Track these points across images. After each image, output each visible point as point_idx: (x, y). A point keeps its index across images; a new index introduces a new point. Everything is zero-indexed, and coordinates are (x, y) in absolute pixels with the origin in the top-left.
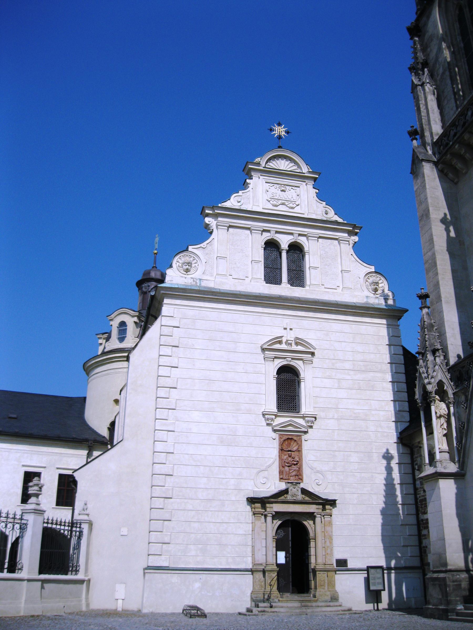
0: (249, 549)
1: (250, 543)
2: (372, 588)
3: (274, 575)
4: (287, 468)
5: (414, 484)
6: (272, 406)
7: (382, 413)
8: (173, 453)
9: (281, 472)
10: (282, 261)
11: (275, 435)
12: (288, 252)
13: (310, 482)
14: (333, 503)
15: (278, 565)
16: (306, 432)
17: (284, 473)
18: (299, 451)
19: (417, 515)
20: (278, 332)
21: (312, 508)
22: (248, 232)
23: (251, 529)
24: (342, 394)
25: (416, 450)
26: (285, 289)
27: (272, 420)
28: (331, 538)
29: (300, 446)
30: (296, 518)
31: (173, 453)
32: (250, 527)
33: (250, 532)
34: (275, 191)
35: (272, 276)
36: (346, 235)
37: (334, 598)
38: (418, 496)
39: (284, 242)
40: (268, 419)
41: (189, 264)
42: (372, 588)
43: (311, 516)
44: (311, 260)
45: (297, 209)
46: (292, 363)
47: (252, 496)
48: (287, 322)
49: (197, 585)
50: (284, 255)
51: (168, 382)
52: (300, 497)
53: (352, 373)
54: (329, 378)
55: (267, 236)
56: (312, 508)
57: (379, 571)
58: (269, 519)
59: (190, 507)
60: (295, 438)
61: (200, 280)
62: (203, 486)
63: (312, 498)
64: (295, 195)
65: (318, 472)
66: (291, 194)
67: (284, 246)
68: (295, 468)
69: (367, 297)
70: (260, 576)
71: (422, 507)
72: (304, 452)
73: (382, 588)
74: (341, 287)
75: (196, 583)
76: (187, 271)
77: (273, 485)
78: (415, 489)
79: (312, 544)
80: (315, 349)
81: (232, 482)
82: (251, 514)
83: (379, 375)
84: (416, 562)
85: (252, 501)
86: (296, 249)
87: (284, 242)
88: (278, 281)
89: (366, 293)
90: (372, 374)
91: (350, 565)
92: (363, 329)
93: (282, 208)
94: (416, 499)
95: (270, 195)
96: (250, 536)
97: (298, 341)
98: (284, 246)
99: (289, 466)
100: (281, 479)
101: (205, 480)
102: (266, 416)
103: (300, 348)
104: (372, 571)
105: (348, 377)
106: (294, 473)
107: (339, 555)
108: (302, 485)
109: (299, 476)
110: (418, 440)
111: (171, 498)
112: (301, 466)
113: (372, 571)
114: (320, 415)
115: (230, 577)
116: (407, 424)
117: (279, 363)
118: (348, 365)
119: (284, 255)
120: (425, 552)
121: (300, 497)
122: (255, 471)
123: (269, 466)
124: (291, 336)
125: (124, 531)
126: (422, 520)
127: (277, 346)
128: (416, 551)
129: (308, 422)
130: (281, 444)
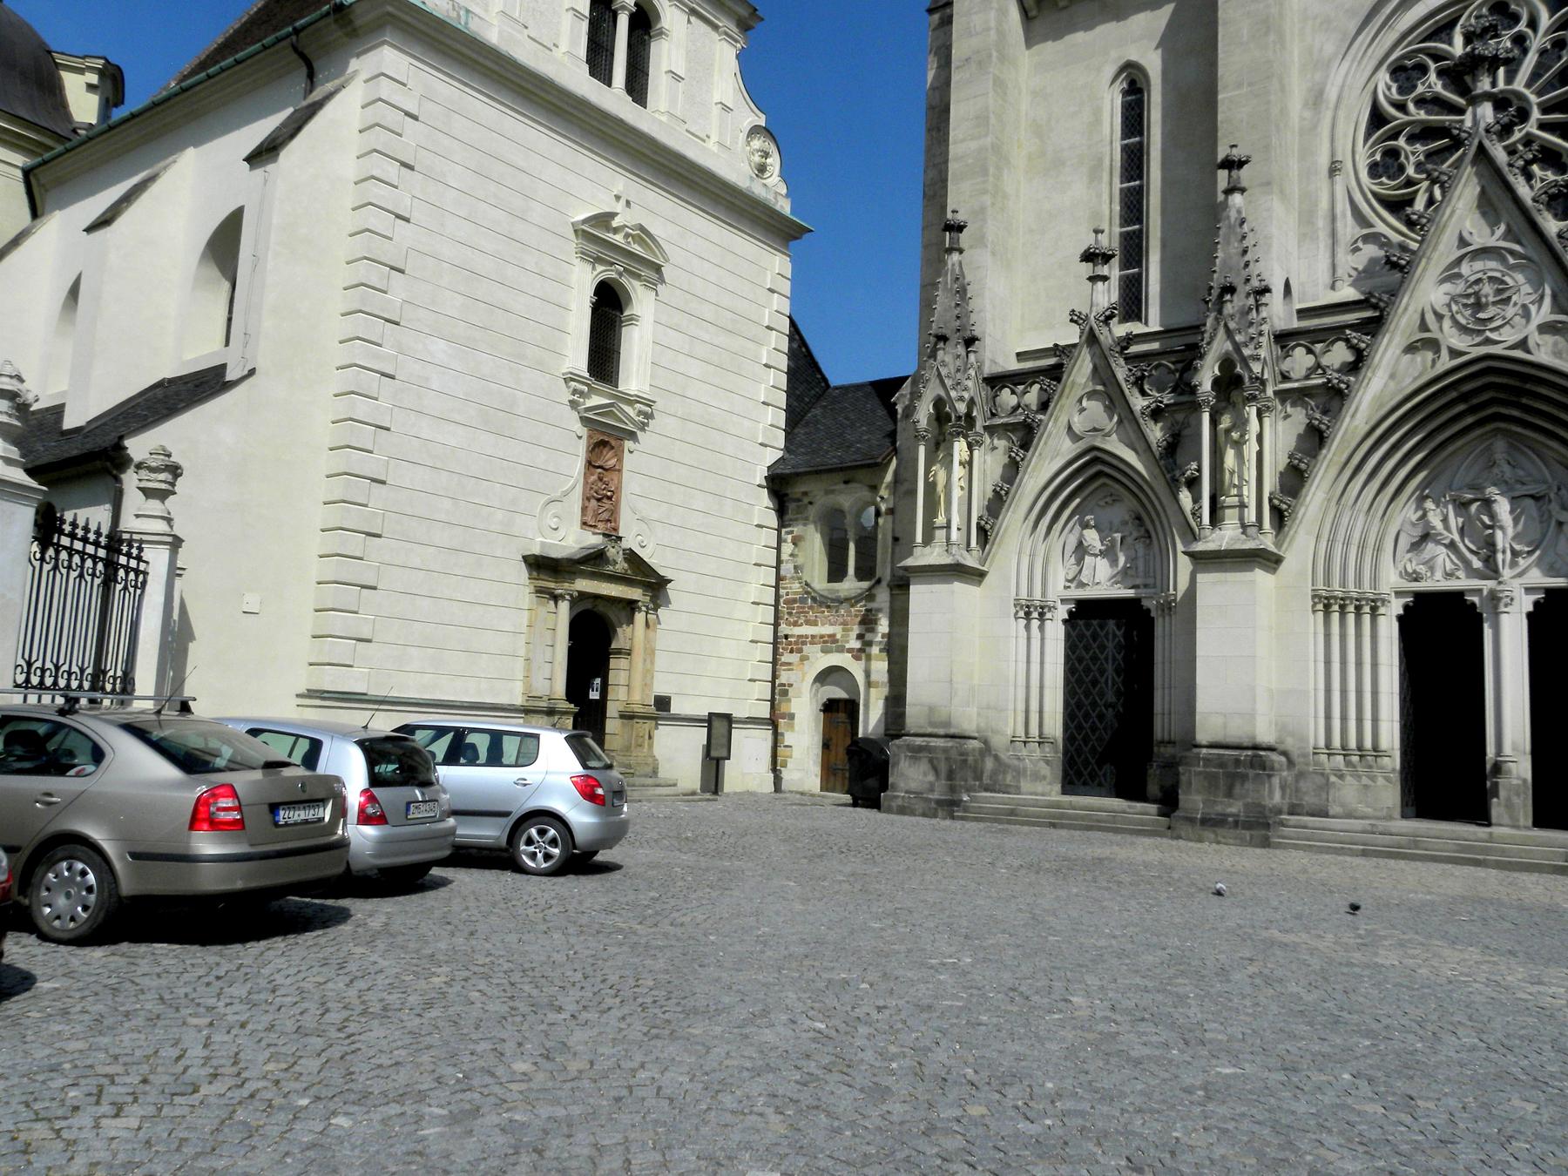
0: (520, 664)
1: (522, 652)
2: (714, 754)
4: (594, 503)
5: (778, 568)
7: (747, 423)
8: (388, 429)
9: (584, 509)
11: (584, 432)
16: (632, 436)
17: (590, 513)
19: (776, 625)
21: (634, 593)
23: (526, 623)
25: (792, 506)
26: (613, 98)
27: (581, 394)
29: (620, 460)
30: (601, 608)
31: (388, 429)
33: (525, 629)
38: (782, 592)
40: (575, 392)
42: (714, 754)
43: (631, 606)
46: (624, 280)
47: (536, 551)
52: (621, 566)
53: (712, 329)
56: (634, 593)
57: (725, 723)
58: (564, 607)
59: (416, 562)
60: (613, 443)
61: (468, 11)
62: (443, 517)
68: (607, 504)
71: (790, 614)
73: (724, 754)
74: (714, 138)
78: (779, 578)
80: (667, 261)
81: (499, 515)
82: (528, 590)
83: (750, 345)
84: (764, 711)
91: (675, 709)
94: (777, 596)
96: (522, 639)
99: (599, 500)
100: (584, 523)
101: (447, 504)
102: (573, 384)
103: (636, 248)
105: (706, 337)
106: (605, 516)
107: (660, 689)
108: (625, 544)
110: (803, 489)
111: (379, 536)
112: (618, 501)
113: (716, 723)
116: (780, 454)
117: (602, 272)
118: (708, 312)
120: (785, 693)
123: (566, 494)
125: (252, 601)
126: (786, 637)
128: (765, 690)
129: (640, 413)
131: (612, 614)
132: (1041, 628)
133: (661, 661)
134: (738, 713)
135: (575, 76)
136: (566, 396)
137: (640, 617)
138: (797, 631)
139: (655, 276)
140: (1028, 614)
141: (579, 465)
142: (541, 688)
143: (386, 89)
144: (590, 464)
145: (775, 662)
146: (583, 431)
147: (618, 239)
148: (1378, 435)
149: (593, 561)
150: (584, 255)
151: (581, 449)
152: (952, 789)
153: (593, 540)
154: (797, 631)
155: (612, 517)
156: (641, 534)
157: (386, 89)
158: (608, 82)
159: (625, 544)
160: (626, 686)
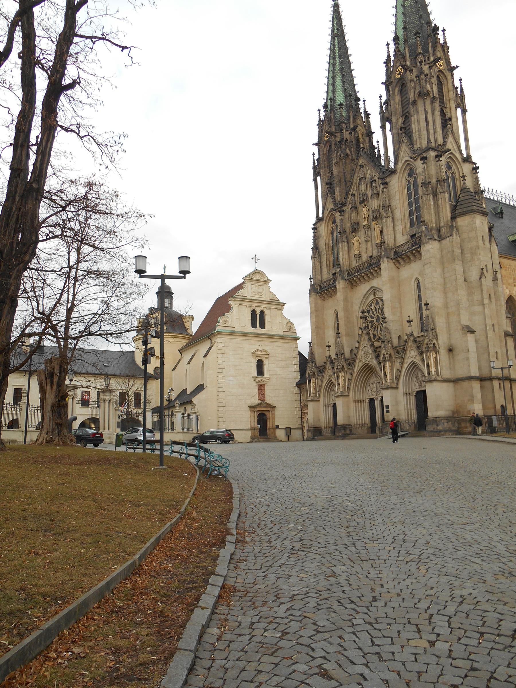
6: (255, 374)
10: (258, 319)
13: (268, 400)
14: (275, 407)
21: (269, 409)
24: (278, 369)
34: (255, 288)
36: (280, 307)
37: (276, 437)
43: (269, 411)
44: (267, 318)
48: (260, 343)
50: (258, 316)
51: (222, 367)
52: (265, 405)
54: (274, 363)
56: (269, 409)
58: (255, 413)
63: (269, 405)
66: (260, 290)
67: (258, 312)
70: (253, 431)
77: (256, 401)
79: (268, 421)
85: (250, 407)
86: (262, 313)
88: (256, 327)
92: (285, 345)
95: (253, 290)
97: (264, 351)
98: (258, 312)
103: (264, 353)
109: (264, 398)
114: (271, 377)
115: (244, 432)
117: (258, 359)
118: (280, 359)
119: (258, 316)
121: (265, 405)
124: (261, 349)
127: (257, 353)
130: (258, 388)
131: (266, 413)
132: (364, 404)
133: (276, 419)
135: (251, 330)
137: (270, 413)
138: (304, 411)
139: (267, 356)
140: (407, 395)
141: (257, 390)
142: (253, 425)
143: (219, 344)
144: (259, 390)
145: (302, 417)
146: (256, 384)
147: (259, 353)
148: (358, 374)
149: (259, 405)
150: (254, 357)
151: (257, 387)
153: (260, 402)
154: (304, 411)
156: (270, 399)
157: (219, 344)
158: (256, 327)
160: (269, 425)
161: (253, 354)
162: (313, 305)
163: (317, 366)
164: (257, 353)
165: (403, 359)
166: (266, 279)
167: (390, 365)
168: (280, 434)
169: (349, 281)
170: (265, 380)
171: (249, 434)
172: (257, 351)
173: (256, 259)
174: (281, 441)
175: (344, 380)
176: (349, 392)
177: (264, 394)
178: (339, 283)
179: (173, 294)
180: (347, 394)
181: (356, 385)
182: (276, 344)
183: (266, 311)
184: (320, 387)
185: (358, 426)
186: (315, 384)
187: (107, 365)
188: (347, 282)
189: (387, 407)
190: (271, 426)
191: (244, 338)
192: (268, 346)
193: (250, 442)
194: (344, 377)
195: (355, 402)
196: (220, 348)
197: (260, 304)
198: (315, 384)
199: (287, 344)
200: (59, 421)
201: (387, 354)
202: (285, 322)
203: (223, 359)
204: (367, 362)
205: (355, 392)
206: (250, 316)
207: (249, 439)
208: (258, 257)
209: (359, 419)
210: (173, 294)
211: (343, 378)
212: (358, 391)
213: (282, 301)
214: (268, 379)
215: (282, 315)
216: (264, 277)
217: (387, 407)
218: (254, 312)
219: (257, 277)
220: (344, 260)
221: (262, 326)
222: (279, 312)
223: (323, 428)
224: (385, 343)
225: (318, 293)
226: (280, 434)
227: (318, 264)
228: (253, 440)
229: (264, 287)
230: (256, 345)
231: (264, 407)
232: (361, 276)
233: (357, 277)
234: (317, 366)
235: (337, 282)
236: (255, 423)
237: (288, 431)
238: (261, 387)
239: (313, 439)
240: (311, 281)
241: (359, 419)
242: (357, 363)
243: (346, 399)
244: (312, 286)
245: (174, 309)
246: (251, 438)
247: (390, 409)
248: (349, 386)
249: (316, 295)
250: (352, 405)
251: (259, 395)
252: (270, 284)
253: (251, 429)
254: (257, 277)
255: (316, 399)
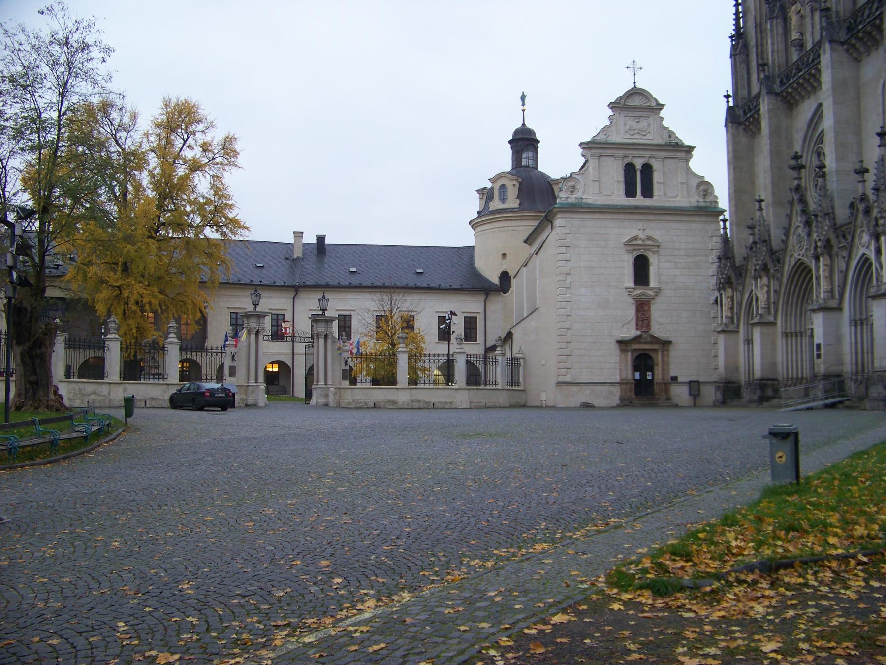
0: (618, 371)
3: (633, 386)
6: (631, 284)
9: (637, 325)
10: (638, 179)
12: (642, 172)
13: (657, 331)
14: (669, 343)
15: (635, 380)
18: (649, 310)
20: (634, 232)
21: (656, 347)
22: (612, 158)
28: (668, 364)
29: (649, 308)
32: (618, 358)
34: (631, 123)
35: (630, 192)
36: (683, 154)
37: (669, 399)
39: (638, 164)
41: (573, 187)
43: (656, 350)
44: (657, 177)
45: (649, 137)
47: (620, 339)
48: (640, 225)
49: (588, 392)
51: (565, 270)
54: (669, 261)
55: (627, 160)
56: (656, 347)
58: (629, 354)
63: (655, 340)
64: (646, 124)
65: (660, 324)
66: (643, 124)
67: (639, 167)
69: (698, 202)
70: (624, 386)
72: (652, 312)
75: (587, 390)
76: (572, 192)
77: (632, 332)
85: (620, 342)
86: (647, 169)
87: (638, 164)
89: (697, 198)
90: (699, 258)
91: (680, 380)
92: (694, 226)
93: (636, 137)
95: (627, 127)
98: (639, 167)
100: (637, 329)
103: (649, 243)
104: (692, 384)
107: (673, 373)
114: (664, 287)
115: (606, 387)
117: (636, 254)
118: (682, 253)
121: (649, 339)
122: (620, 324)
125: (543, 362)
127: (634, 243)
131: (651, 354)
133: (672, 367)
134: (701, 379)
136: (626, 294)
137: (660, 353)
139: (655, 249)
142: (624, 376)
144: (638, 311)
146: (632, 301)
147: (640, 242)
149: (636, 339)
150: (627, 251)
152: (724, 398)
153: (639, 333)
155: (648, 326)
159: (651, 332)
161: (628, 244)
162: (731, 147)
163: (737, 264)
164: (634, 243)
165: (850, 248)
166: (654, 104)
167: (829, 262)
168: (680, 393)
169: (782, 96)
170: (651, 293)
171: (617, 391)
172: (635, 238)
173: (634, 68)
174: (676, 406)
175: (768, 292)
176: (775, 318)
177: (648, 319)
178: (764, 101)
179: (539, 142)
180: (771, 319)
181: (787, 303)
182: (675, 225)
183: (656, 165)
184: (740, 304)
185: (789, 382)
186: (733, 300)
187: (421, 271)
188: (779, 98)
189: (818, 346)
190: (660, 377)
191: (609, 216)
192: (657, 230)
193: (618, 406)
194: (768, 286)
195: (786, 335)
196: (562, 236)
197: (641, 152)
198: (733, 300)
199: (698, 226)
200: (33, 378)
201: (819, 240)
202: (694, 182)
203: (568, 256)
204: (800, 257)
205: (786, 315)
206: (621, 177)
207: (616, 401)
208: (639, 64)
209: (797, 369)
210: (539, 142)
211: (766, 289)
212: (791, 315)
213: (687, 142)
214: (658, 291)
215: (688, 169)
216: (649, 101)
217: (818, 346)
218: (629, 168)
219: (637, 102)
220: (776, 54)
221: (648, 192)
222: (682, 164)
223: (743, 383)
224: (819, 219)
225: (740, 124)
226: (680, 393)
227: (743, 66)
228: (625, 403)
229: (651, 119)
230: (632, 229)
231: (646, 343)
232: (799, 84)
233: (792, 87)
234: (737, 264)
235: (761, 100)
236: (628, 373)
237: (695, 387)
238: (643, 308)
239: (723, 403)
240: (728, 102)
241: (797, 369)
242: (787, 258)
243: (768, 330)
244: (730, 110)
245: (541, 168)
246: (620, 399)
247: (822, 352)
248: (776, 304)
249: (737, 129)
250: (780, 341)
251: (637, 321)
252: (662, 114)
253: (620, 384)
254: (637, 102)
255: (732, 328)
